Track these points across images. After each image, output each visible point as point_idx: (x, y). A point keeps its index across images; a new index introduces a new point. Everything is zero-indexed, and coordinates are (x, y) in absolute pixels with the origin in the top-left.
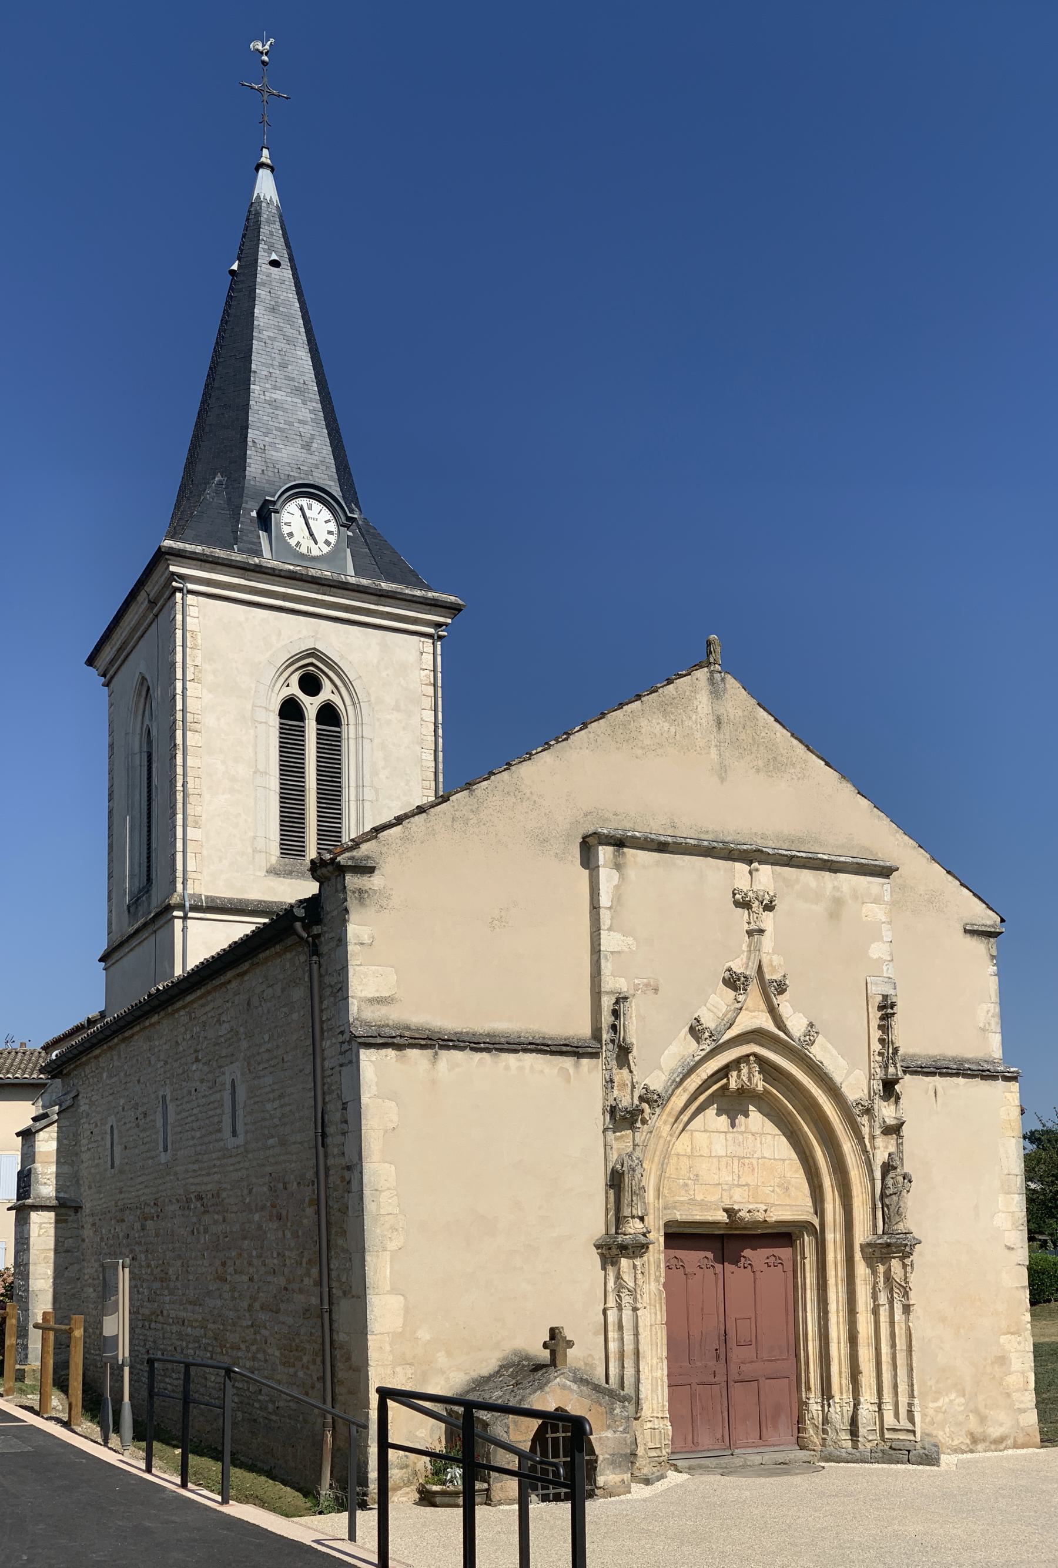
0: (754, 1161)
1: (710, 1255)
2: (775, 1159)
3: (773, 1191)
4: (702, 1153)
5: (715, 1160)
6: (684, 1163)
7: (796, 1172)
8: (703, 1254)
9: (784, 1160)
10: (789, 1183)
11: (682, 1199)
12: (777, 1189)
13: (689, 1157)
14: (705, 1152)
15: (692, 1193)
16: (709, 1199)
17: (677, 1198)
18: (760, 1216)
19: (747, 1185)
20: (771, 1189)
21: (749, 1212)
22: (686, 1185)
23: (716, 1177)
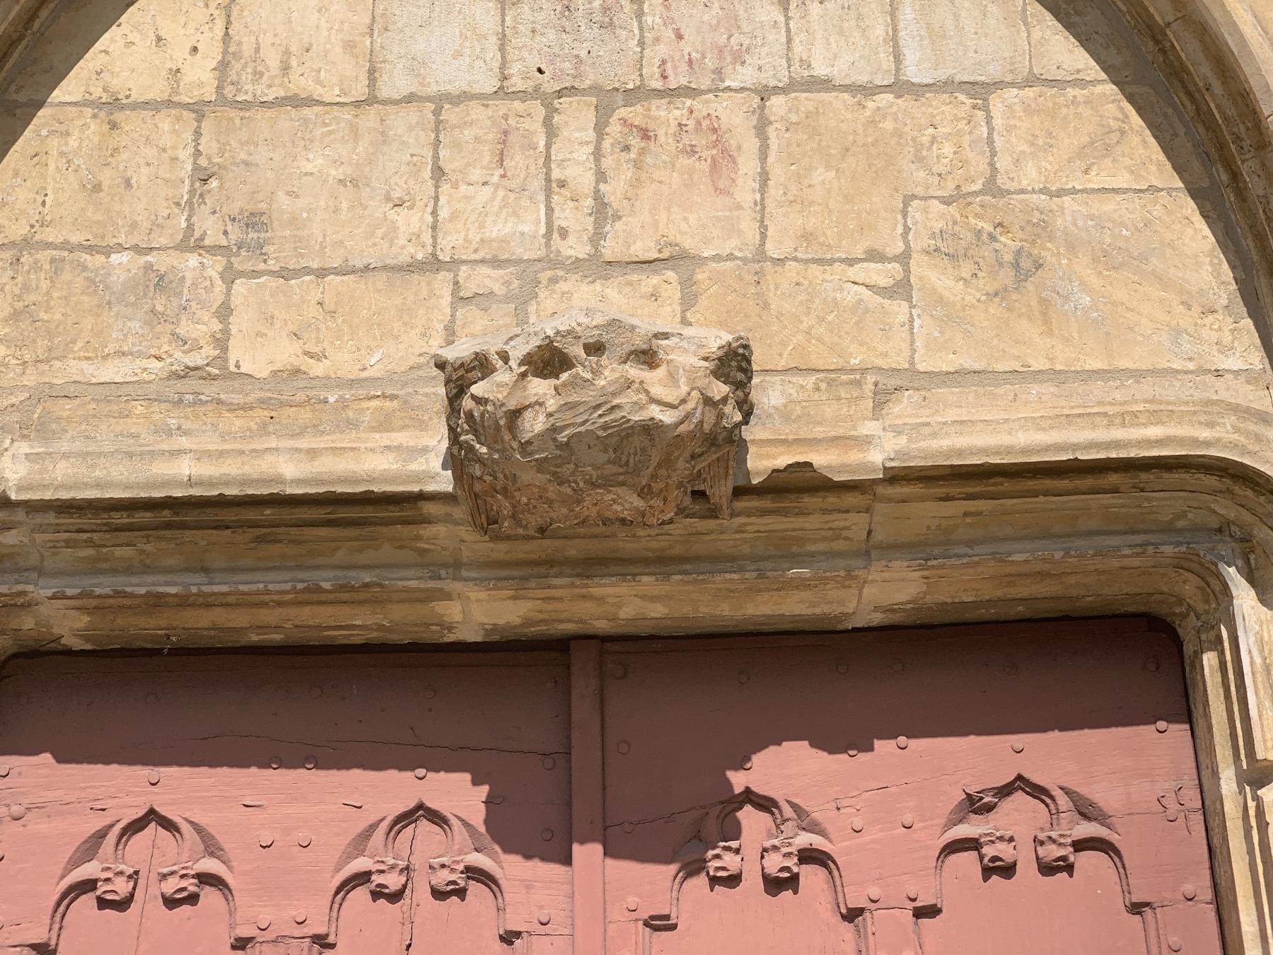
0: (733, 114)
1: (460, 795)
2: (900, 87)
3: (901, 289)
4: (301, 83)
5: (402, 122)
6: (157, 156)
7: (1101, 147)
8: (394, 789)
9: (980, 91)
10: (1041, 228)
11: (112, 372)
12: (932, 276)
13: (199, 110)
14: (335, 75)
15: (202, 327)
16: (341, 361)
17: (74, 369)
18: (668, 395)
19: (674, 259)
20: (881, 274)
21: (548, 361)
22: (162, 283)
23: (412, 221)
